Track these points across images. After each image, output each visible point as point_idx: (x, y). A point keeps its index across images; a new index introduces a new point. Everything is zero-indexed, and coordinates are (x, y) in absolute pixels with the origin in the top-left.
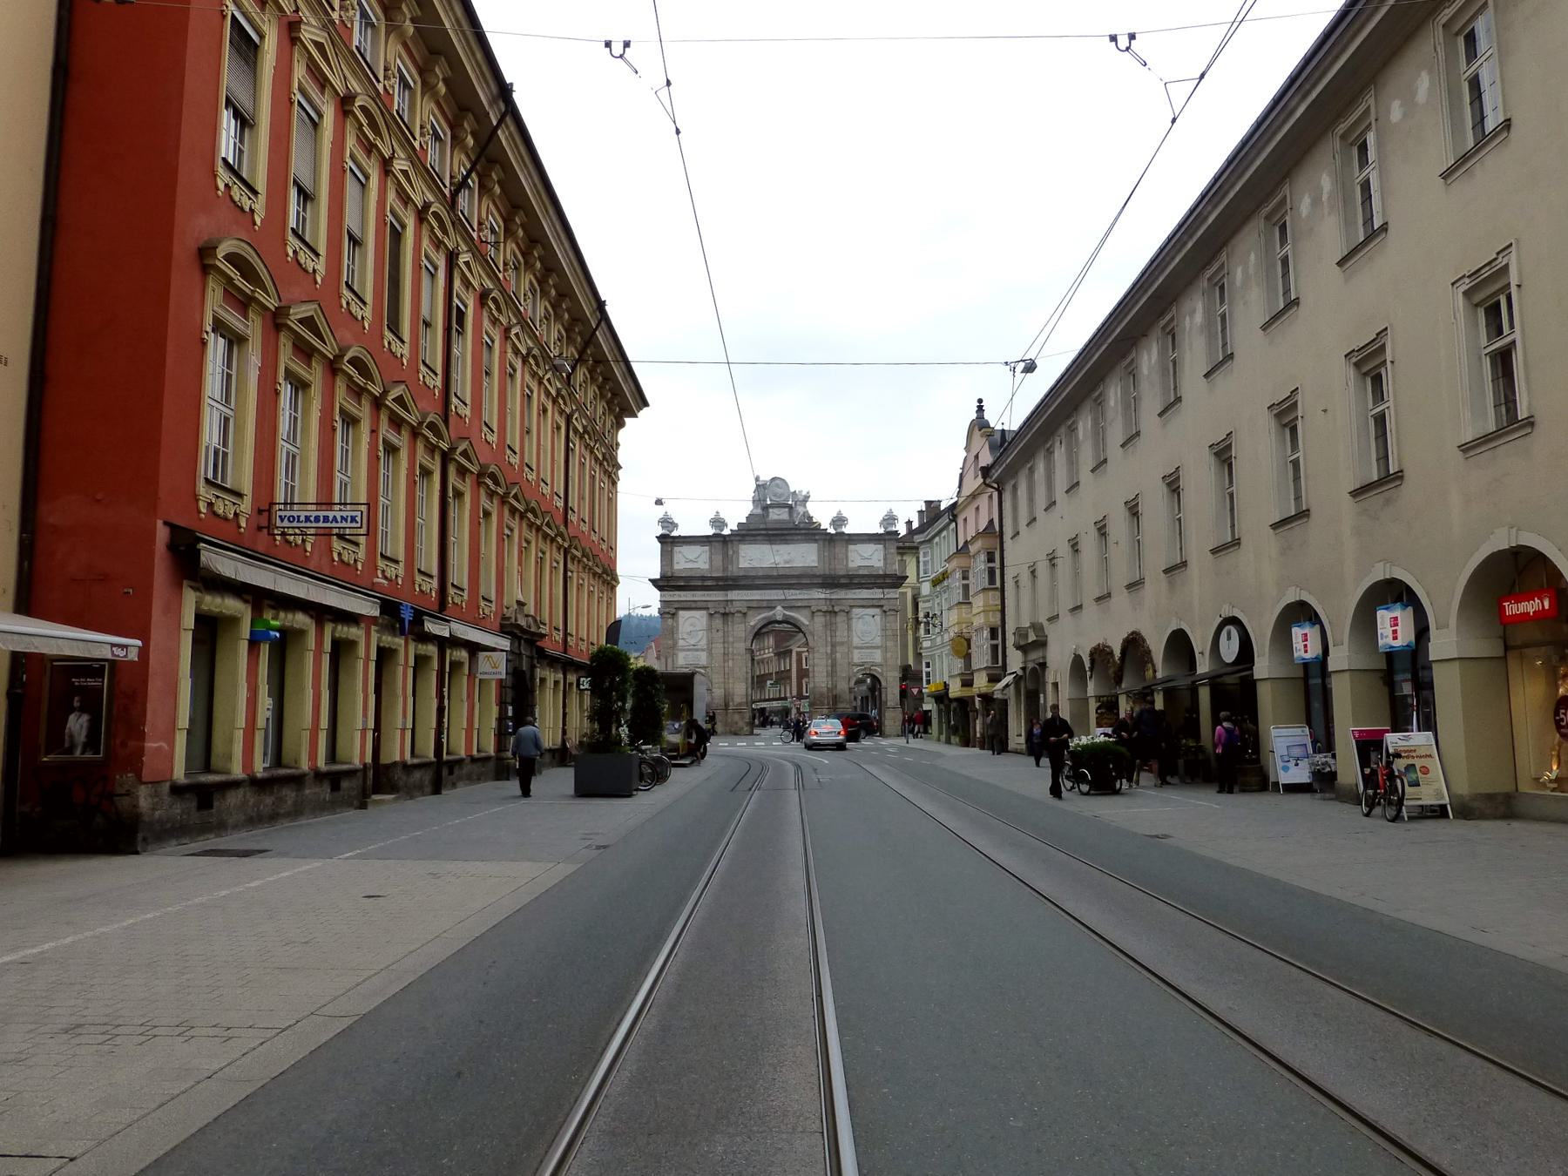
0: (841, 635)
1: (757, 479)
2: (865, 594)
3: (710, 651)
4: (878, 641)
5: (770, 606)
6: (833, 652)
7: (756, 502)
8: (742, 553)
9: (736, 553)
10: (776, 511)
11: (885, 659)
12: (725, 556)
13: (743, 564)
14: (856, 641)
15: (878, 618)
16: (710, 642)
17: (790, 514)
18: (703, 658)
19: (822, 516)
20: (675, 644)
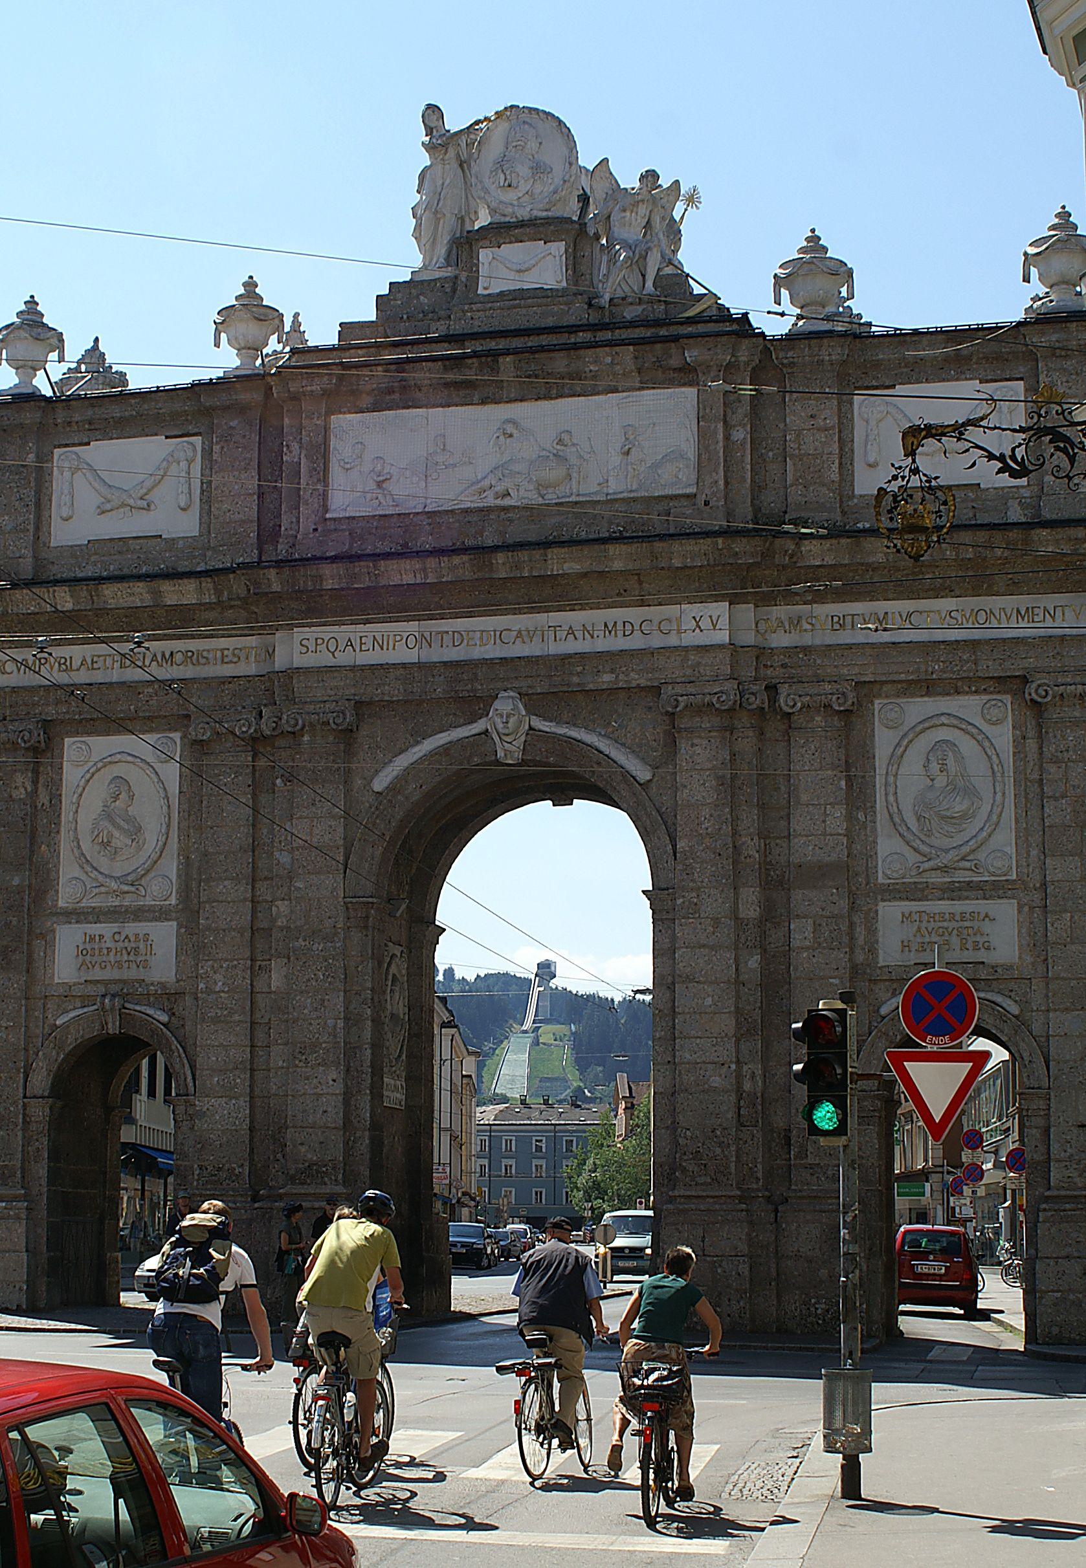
0: (817, 829)
1: (432, 113)
2: (940, 618)
3: (189, 911)
4: (1003, 852)
5: (466, 688)
6: (773, 914)
7: (426, 219)
8: (341, 449)
9: (321, 453)
10: (512, 252)
11: (1038, 943)
12: (271, 465)
13: (349, 495)
14: (891, 855)
15: (1004, 737)
16: (194, 876)
17: (575, 264)
18: (161, 951)
19: (734, 266)
20: (42, 881)
